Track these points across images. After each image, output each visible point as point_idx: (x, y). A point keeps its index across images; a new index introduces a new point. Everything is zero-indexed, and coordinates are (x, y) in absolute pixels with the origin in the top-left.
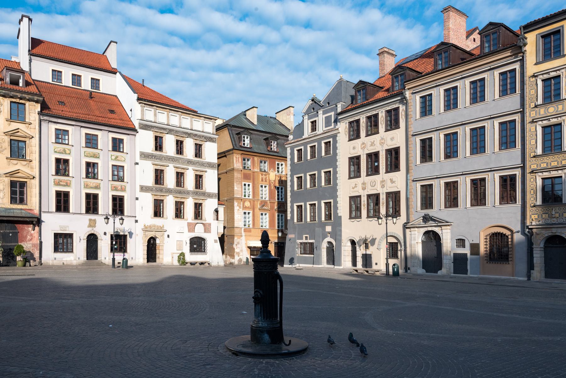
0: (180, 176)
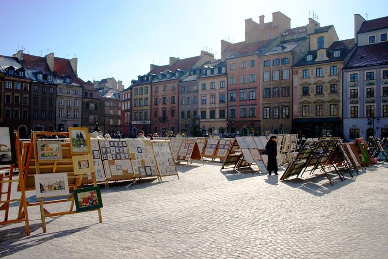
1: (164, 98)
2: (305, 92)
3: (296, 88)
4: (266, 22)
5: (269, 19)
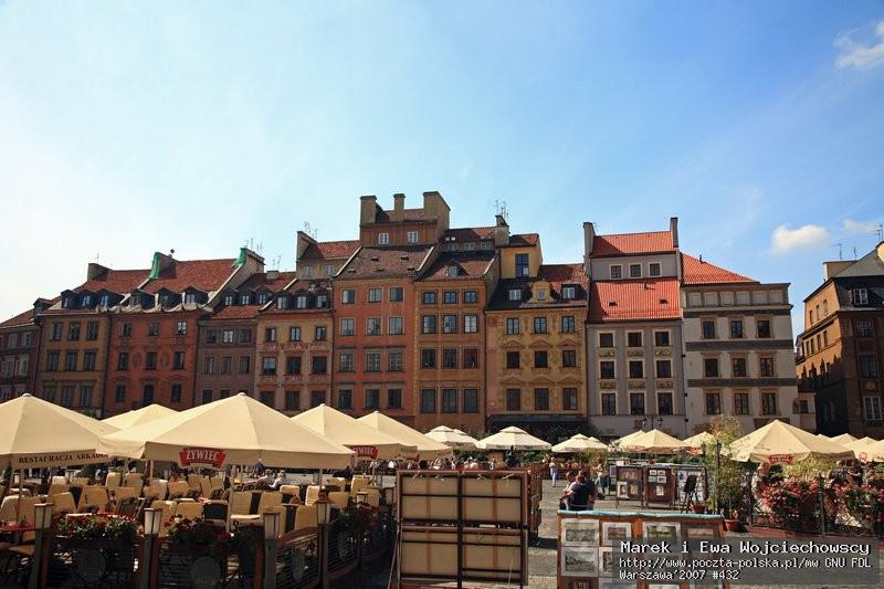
0: (740, 367)
1: (151, 355)
2: (513, 360)
3: (494, 351)
4: (408, 206)
5: (414, 202)
